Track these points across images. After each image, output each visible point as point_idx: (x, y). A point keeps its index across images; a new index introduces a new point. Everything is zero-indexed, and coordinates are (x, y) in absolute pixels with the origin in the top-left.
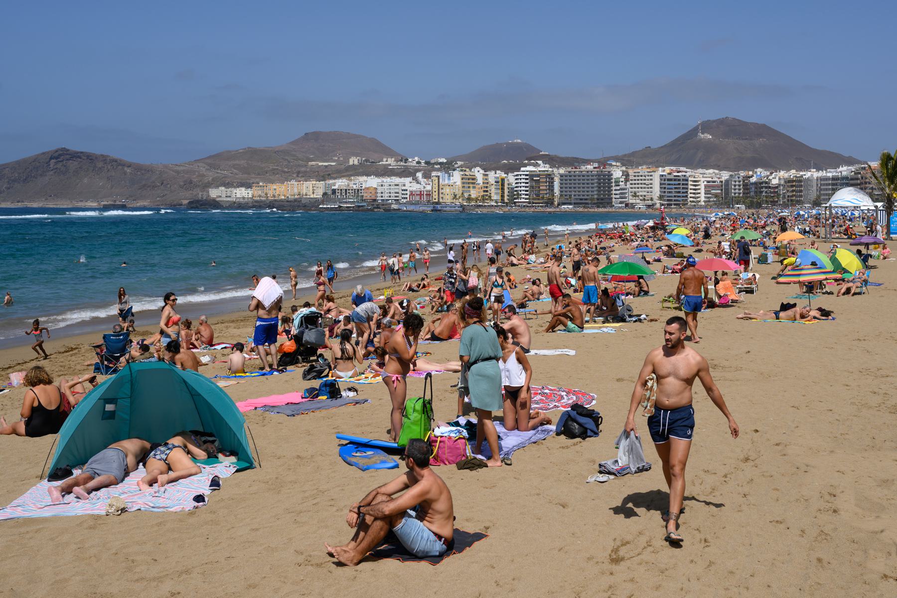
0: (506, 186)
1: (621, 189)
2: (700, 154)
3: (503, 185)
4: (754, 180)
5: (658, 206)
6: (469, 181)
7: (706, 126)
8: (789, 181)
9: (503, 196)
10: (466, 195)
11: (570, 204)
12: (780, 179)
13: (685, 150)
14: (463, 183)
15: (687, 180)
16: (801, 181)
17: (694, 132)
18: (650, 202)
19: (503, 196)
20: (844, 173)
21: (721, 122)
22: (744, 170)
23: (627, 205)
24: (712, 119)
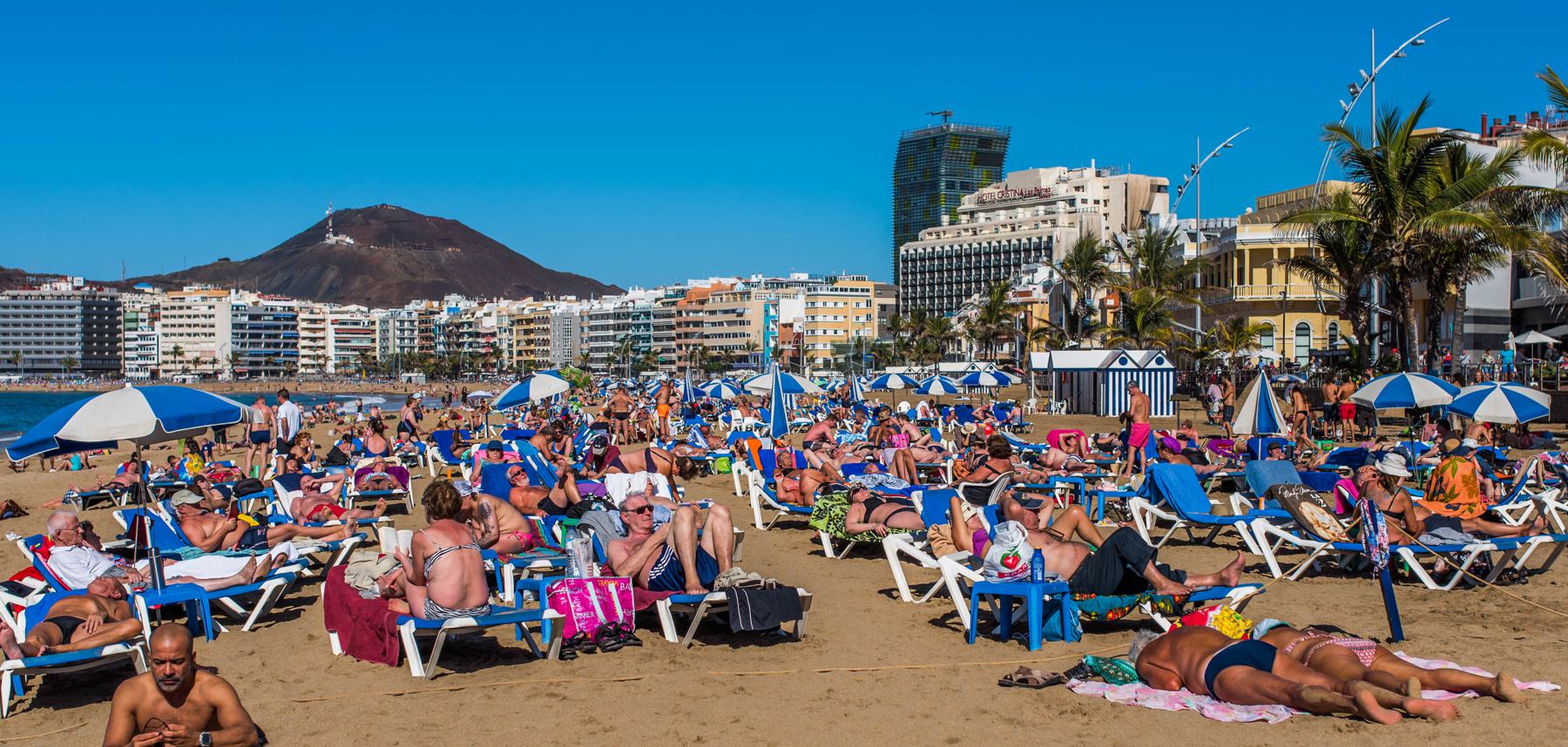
1: (143, 337)
2: (331, 275)
4: (443, 318)
5: (226, 375)
7: (342, 221)
8: (519, 322)
11: (16, 371)
12: (500, 317)
13: (298, 267)
15: (294, 318)
16: (546, 320)
17: (319, 231)
18: (208, 368)
20: (639, 304)
21: (372, 213)
22: (421, 297)
23: (154, 374)
24: (353, 207)
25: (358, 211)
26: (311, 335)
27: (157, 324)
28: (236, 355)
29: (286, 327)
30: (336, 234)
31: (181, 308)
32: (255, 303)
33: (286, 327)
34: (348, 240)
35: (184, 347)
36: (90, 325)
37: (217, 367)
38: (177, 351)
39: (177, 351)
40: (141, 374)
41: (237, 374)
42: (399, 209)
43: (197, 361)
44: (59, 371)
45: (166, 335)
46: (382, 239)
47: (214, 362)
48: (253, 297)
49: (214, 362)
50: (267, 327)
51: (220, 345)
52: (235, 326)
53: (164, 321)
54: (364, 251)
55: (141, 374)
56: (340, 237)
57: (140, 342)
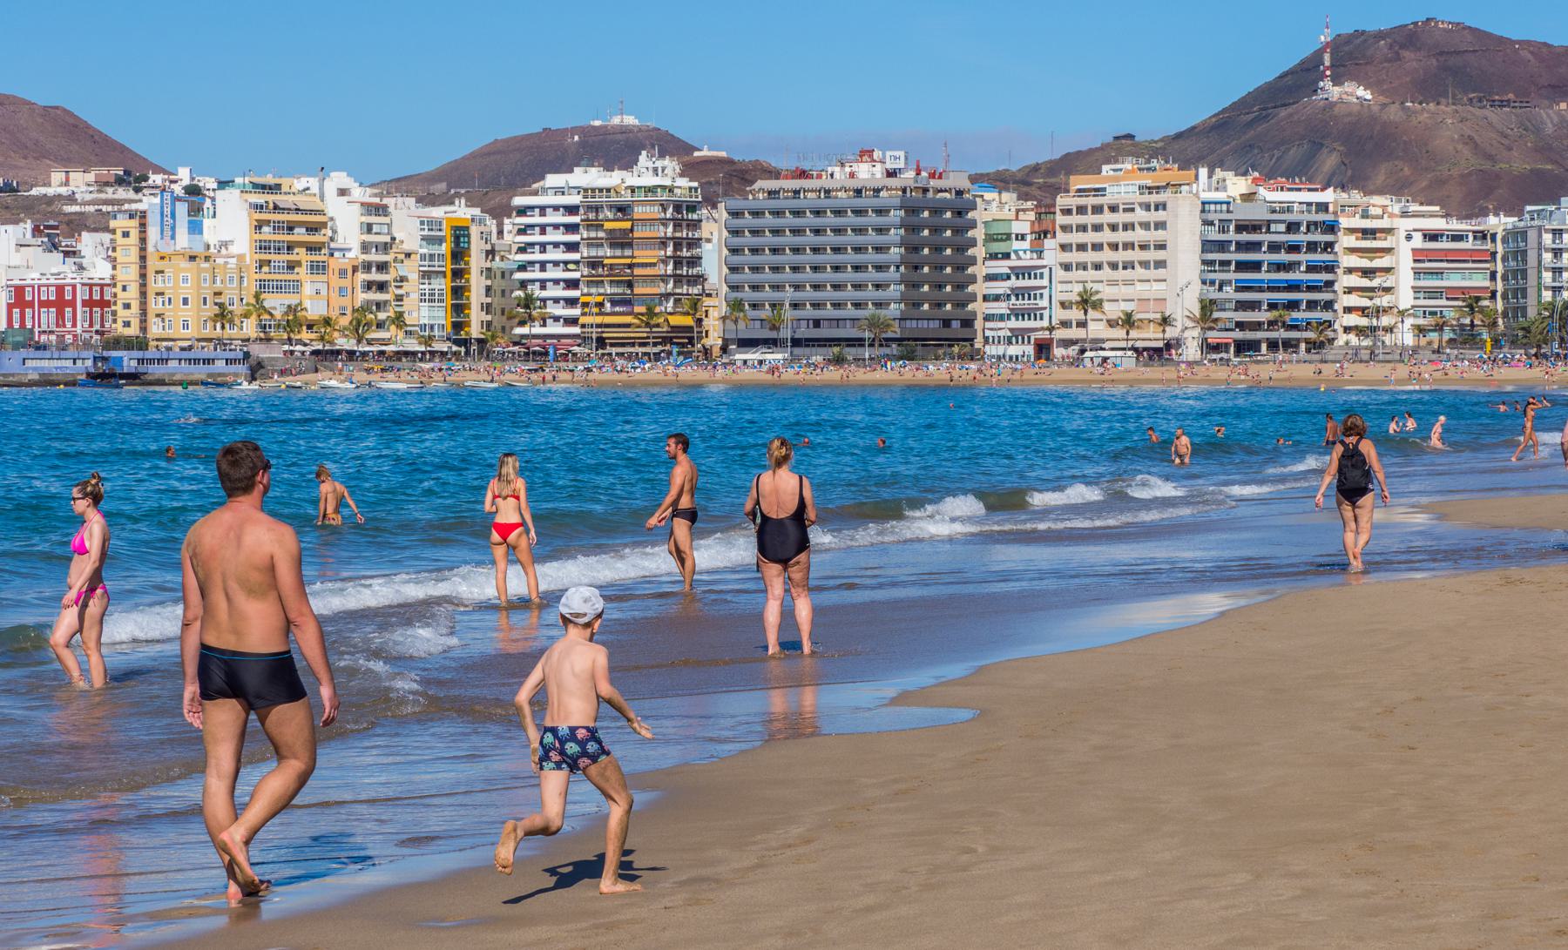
0: (476, 261)
1: (1020, 272)
3: (459, 254)
5: (1191, 351)
6: (293, 235)
7: (1349, 55)
9: (459, 309)
10: (276, 303)
14: (263, 247)
17: (1303, 77)
18: (1150, 336)
19: (459, 309)
21: (1408, 37)
24: (1372, 26)
25: (1380, 35)
26: (1365, 263)
27: (1049, 243)
28: (1208, 306)
29: (1312, 247)
30: (1337, 81)
31: (1098, 210)
32: (1249, 197)
33: (1312, 247)
34: (1361, 92)
35: (1106, 292)
36: (916, 249)
37: (1171, 333)
38: (1087, 302)
39: (1087, 302)
40: (1013, 350)
41: (1211, 348)
42: (1461, 28)
43: (1128, 321)
44: (858, 342)
45: (1067, 267)
46: (1429, 88)
47: (1165, 321)
48: (1237, 185)
49: (1165, 321)
50: (1274, 247)
51: (1180, 285)
52: (1207, 245)
53: (1062, 237)
54: (1393, 113)
55: (1013, 350)
56: (1349, 87)
57: (1014, 282)
